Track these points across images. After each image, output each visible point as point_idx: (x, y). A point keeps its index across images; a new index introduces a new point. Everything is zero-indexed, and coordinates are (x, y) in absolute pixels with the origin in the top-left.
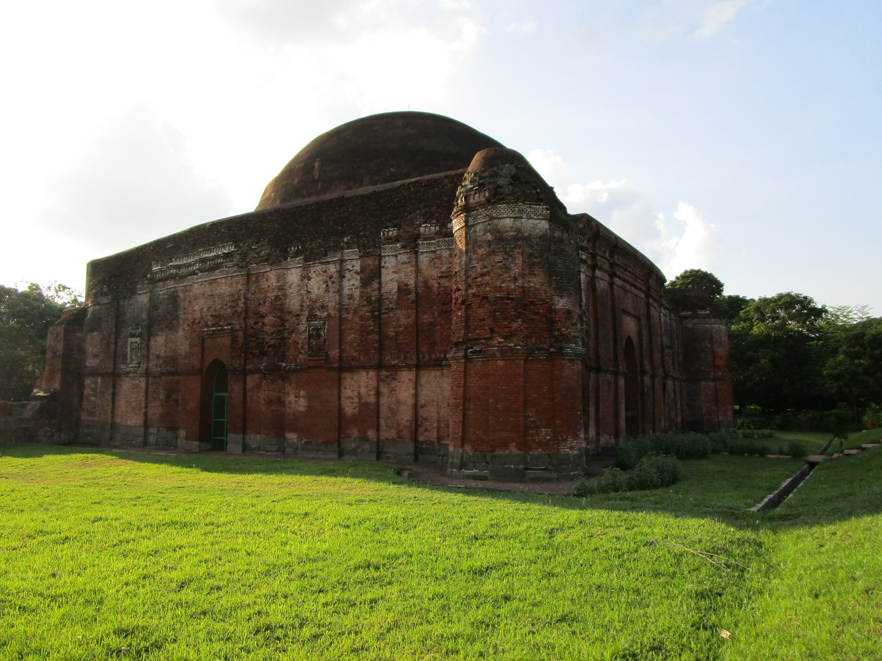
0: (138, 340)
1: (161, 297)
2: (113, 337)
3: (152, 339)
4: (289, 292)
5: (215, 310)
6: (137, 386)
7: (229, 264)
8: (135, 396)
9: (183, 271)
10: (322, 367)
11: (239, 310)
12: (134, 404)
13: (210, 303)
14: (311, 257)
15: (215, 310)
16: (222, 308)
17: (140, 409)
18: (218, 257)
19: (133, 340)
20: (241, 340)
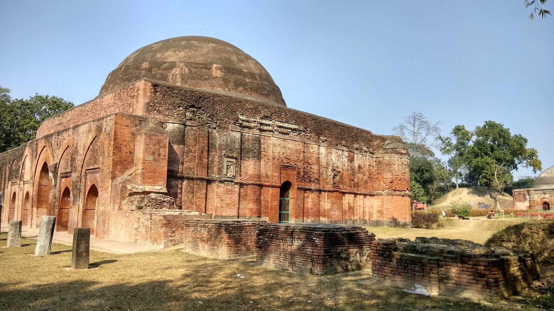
0: (234, 160)
1: (246, 137)
2: (205, 153)
3: (242, 162)
4: (320, 156)
5: (287, 156)
6: (231, 190)
7: (294, 134)
8: (230, 196)
9: (265, 128)
10: (338, 191)
11: (301, 159)
12: (229, 202)
13: (284, 151)
14: (330, 145)
15: (287, 156)
16: (291, 155)
17: (235, 205)
18: (289, 128)
19: (230, 160)
20: (302, 174)
